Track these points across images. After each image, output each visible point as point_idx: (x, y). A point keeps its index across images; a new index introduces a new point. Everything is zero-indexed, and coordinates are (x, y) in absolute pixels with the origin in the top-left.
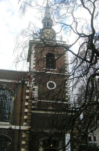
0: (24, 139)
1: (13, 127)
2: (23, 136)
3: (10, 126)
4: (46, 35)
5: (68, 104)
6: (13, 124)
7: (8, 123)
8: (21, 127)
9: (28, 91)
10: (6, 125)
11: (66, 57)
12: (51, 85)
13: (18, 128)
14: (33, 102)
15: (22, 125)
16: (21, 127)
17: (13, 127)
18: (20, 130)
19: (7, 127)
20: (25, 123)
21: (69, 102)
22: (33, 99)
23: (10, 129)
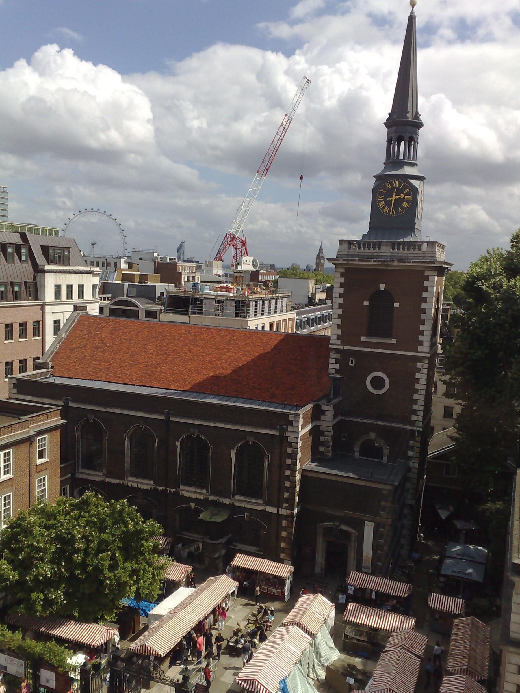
0: (285, 529)
1: (269, 509)
2: (283, 524)
3: (264, 507)
4: (386, 207)
5: (414, 431)
6: (267, 505)
7: (261, 502)
8: (280, 509)
9: (289, 450)
10: (258, 504)
11: (427, 301)
12: (378, 383)
13: (274, 510)
14: (322, 439)
15: (282, 508)
16: (280, 509)
17: (269, 509)
18: (278, 515)
19: (260, 508)
20: (285, 505)
21: (417, 427)
22: (322, 433)
23: (264, 511)
